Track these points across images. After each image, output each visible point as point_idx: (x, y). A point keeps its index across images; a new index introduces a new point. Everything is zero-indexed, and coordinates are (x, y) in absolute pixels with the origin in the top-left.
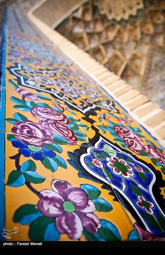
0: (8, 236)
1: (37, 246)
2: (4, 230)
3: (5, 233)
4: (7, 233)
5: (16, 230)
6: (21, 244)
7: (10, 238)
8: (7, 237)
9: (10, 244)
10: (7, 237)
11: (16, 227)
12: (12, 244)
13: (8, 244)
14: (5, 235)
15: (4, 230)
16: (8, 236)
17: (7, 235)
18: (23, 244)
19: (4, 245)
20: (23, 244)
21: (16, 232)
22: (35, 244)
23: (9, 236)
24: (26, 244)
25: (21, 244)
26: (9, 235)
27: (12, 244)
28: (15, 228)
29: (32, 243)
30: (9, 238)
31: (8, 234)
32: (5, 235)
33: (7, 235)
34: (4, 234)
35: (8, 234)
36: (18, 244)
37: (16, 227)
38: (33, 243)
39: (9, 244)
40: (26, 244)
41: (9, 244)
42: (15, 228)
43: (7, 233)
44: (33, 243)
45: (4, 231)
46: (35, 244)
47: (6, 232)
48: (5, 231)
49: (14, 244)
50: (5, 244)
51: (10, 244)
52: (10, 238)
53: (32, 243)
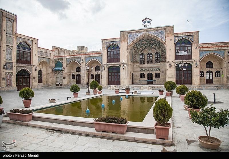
0: (7, 148)
1: (34, 157)
2: (3, 142)
3: (4, 145)
5: (15, 143)
6: (19, 156)
9: (9, 156)
11: (14, 140)
12: (11, 156)
13: (7, 156)
14: (4, 147)
15: (3, 142)
16: (7, 148)
17: (6, 147)
18: (21, 156)
19: (3, 156)
20: (21, 156)
22: (32, 156)
23: (8, 148)
24: (24, 156)
25: (19, 156)
27: (11, 156)
28: (13, 141)
29: (29, 155)
32: (4, 147)
33: (6, 147)
34: (3, 146)
36: (16, 155)
38: (30, 154)
39: (8, 156)
40: (24, 156)
41: (8, 156)
42: (13, 141)
44: (30, 154)
46: (32, 156)
48: (5, 143)
49: (12, 156)
50: (4, 156)
51: (9, 156)
53: (29, 155)
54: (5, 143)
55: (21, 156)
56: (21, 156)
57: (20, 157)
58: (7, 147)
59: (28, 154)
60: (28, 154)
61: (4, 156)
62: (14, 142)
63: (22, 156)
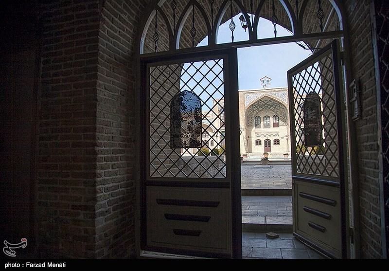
0: (12, 253)
1: (57, 268)
2: (6, 242)
5: (25, 243)
6: (32, 265)
7: (15, 256)
8: (11, 254)
9: (16, 265)
10: (11, 254)
12: (18, 265)
13: (11, 265)
15: (6, 242)
18: (35, 265)
19: (6, 267)
20: (35, 265)
22: (54, 265)
24: (40, 265)
25: (32, 265)
26: (12, 251)
27: (18, 265)
28: (23, 240)
29: (50, 263)
30: (14, 255)
31: (12, 249)
33: (10, 251)
34: (5, 249)
35: (12, 249)
36: (27, 265)
37: (24, 239)
38: (51, 263)
39: (13, 265)
40: (40, 265)
41: (13, 265)
42: (23, 240)
44: (51, 263)
45: (6, 244)
46: (54, 265)
47: (9, 246)
48: (7, 244)
49: (21, 265)
50: (7, 265)
51: (16, 265)
52: (15, 256)
53: (50, 263)
54: (7, 244)
55: (36, 266)
56: (36, 266)
57: (34, 268)
59: (48, 263)
60: (48, 263)
61: (6, 265)
62: (24, 242)
63: (38, 266)
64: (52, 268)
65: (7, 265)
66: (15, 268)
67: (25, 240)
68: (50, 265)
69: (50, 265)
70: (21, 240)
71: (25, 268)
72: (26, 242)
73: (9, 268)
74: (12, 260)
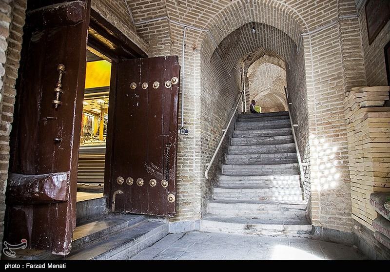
0: (12, 254)
1: (57, 269)
2: (6, 243)
4: (10, 249)
5: (25, 244)
6: (32, 266)
7: (16, 257)
8: (11, 255)
9: (16, 266)
12: (18, 266)
13: (12, 266)
15: (6, 243)
16: (12, 254)
17: (10, 252)
18: (35, 266)
19: (6, 268)
20: (35, 266)
21: (24, 247)
22: (54, 266)
23: (14, 254)
24: (40, 266)
25: (32, 266)
26: (12, 252)
27: (18, 266)
29: (50, 264)
30: (14, 256)
32: (6, 252)
33: (10, 252)
34: (5, 250)
36: (27, 266)
37: (24, 240)
38: (51, 264)
39: (13, 266)
40: (40, 266)
41: (13, 266)
43: (10, 249)
44: (51, 264)
45: (6, 245)
46: (54, 266)
48: (7, 245)
49: (21, 266)
50: (7, 266)
51: (16, 266)
52: (16, 257)
53: (50, 264)
54: (7, 245)
55: (36, 267)
56: (36, 267)
57: (34, 269)
58: (11, 252)
59: (48, 264)
60: (48, 264)
61: (6, 266)
62: (24, 242)
63: (38, 267)
64: (52, 269)
65: (7, 266)
66: (15, 269)
67: (25, 241)
68: (50, 266)
69: (50, 266)
70: (22, 241)
71: (25, 269)
72: (26, 242)
73: (9, 269)
74: (13, 262)
